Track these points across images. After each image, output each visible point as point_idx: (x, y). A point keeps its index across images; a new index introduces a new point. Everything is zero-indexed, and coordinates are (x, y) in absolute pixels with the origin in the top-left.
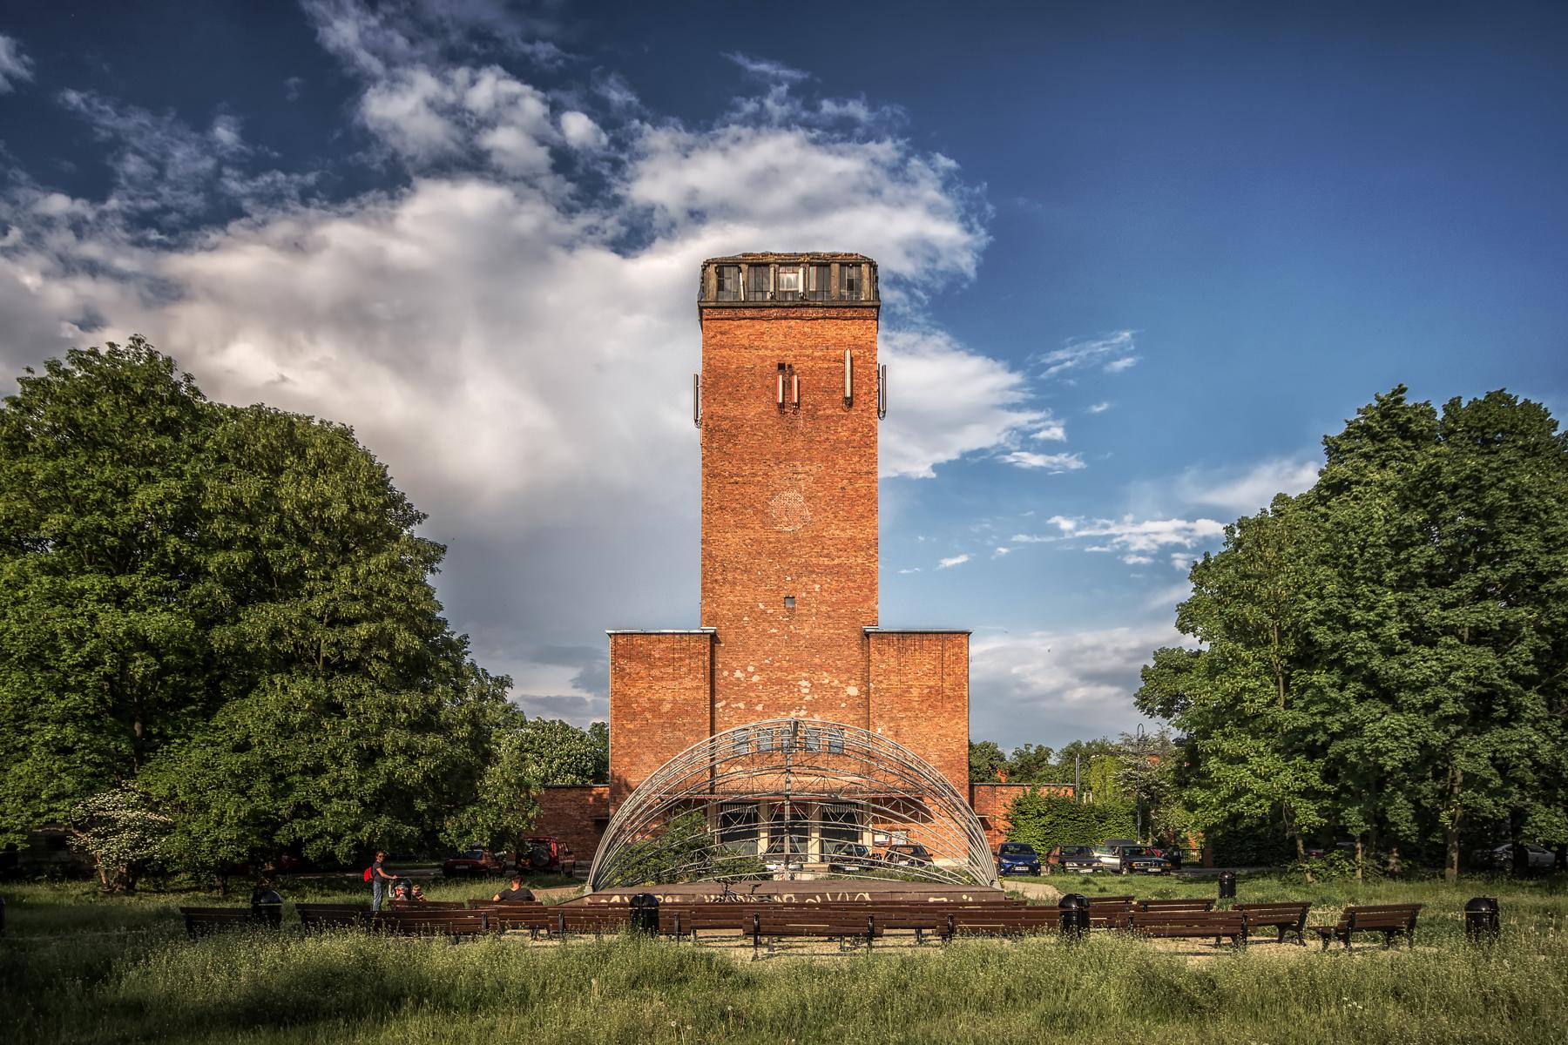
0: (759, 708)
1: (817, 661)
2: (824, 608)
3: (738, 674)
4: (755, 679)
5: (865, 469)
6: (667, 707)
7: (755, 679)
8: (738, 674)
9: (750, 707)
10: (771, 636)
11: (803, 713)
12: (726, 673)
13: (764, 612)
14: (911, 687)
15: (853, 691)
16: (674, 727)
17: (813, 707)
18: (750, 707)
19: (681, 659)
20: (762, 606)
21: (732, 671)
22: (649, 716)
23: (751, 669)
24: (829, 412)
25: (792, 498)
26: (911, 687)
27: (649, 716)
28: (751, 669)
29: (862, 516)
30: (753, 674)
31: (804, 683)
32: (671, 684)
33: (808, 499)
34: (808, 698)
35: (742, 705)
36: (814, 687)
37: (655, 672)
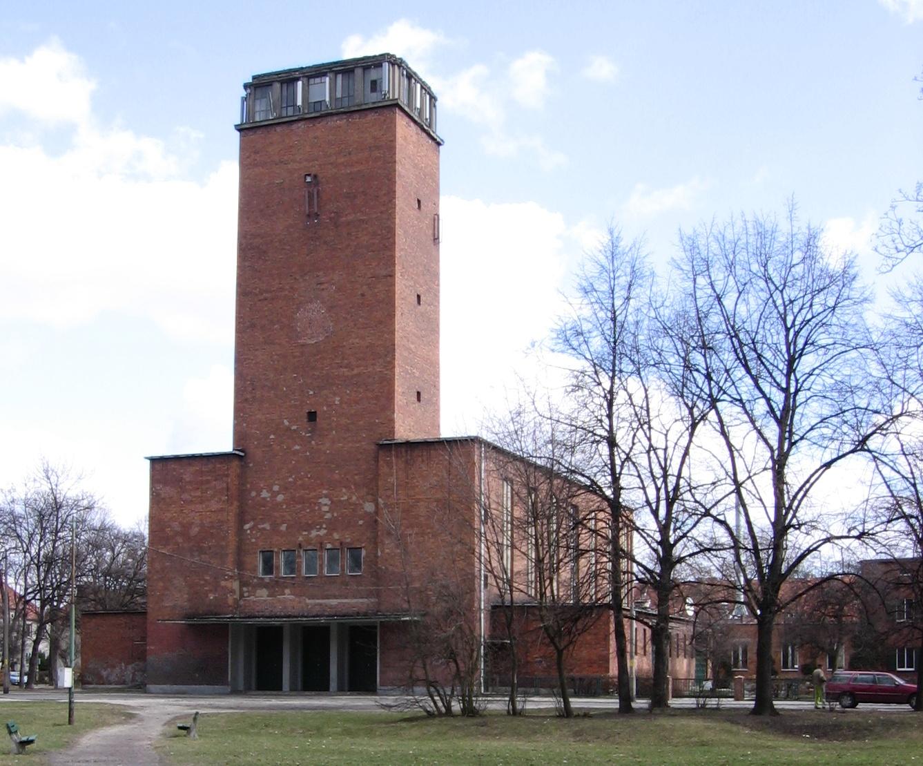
0: (283, 527)
1: (337, 477)
2: (344, 421)
3: (265, 494)
4: (280, 498)
5: (384, 273)
6: (195, 530)
7: (280, 498)
8: (265, 494)
9: (275, 526)
10: (296, 453)
11: (323, 532)
12: (254, 494)
13: (288, 429)
14: (418, 500)
15: (369, 507)
16: (201, 551)
17: (332, 526)
18: (275, 526)
19: (208, 482)
20: (286, 423)
21: (259, 492)
22: (180, 540)
23: (276, 488)
24: (350, 218)
25: (315, 311)
26: (418, 500)
27: (180, 540)
28: (276, 488)
29: (381, 322)
30: (278, 493)
31: (325, 501)
32: (200, 507)
33: (330, 309)
34: (328, 516)
35: (267, 526)
36: (335, 505)
37: (186, 496)
